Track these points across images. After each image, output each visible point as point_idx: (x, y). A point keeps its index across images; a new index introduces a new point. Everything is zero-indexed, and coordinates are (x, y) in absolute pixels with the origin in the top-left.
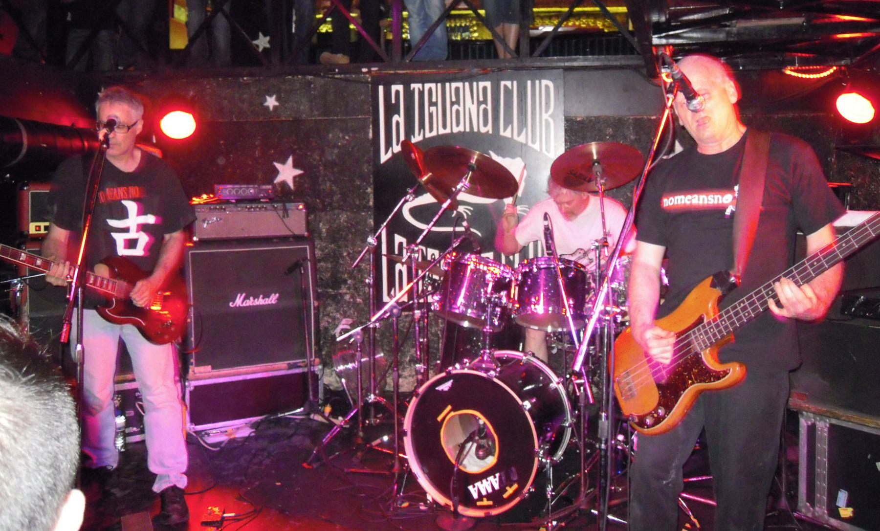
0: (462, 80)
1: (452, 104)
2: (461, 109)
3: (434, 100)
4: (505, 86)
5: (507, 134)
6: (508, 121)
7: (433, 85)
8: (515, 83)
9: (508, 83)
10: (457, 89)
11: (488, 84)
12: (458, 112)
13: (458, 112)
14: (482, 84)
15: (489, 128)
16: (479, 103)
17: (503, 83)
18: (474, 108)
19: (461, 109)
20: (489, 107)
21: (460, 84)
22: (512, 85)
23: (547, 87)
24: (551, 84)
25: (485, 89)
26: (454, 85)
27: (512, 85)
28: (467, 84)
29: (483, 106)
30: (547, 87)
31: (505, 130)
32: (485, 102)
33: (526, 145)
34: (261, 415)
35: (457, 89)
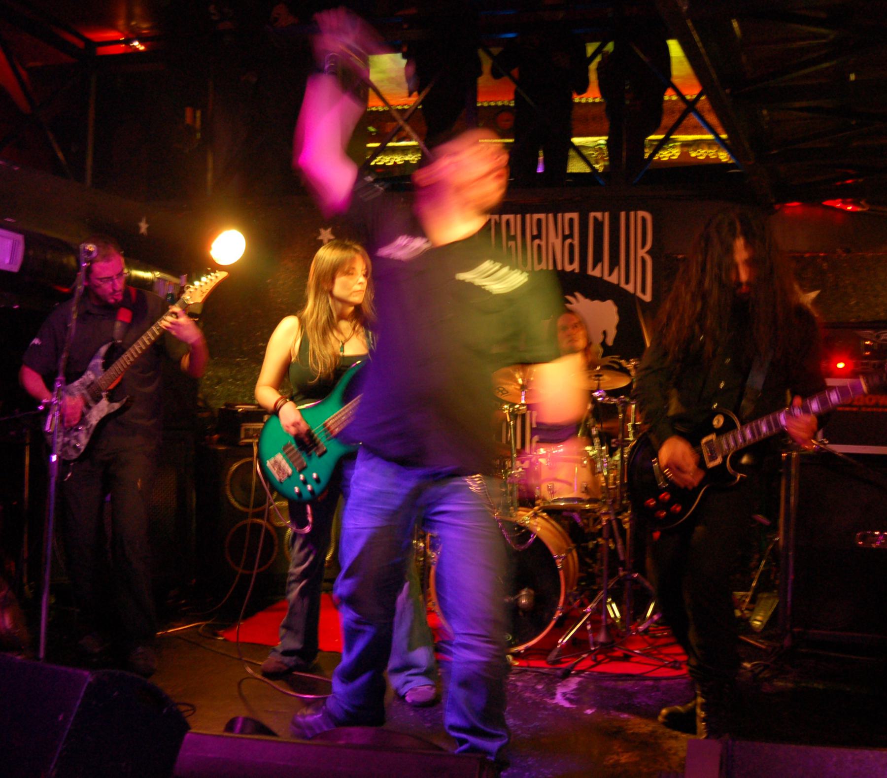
0: (547, 211)
1: (534, 238)
2: (543, 243)
3: (512, 233)
4: (595, 219)
5: (596, 273)
6: (598, 259)
7: (511, 217)
8: (607, 214)
9: (599, 215)
10: (539, 221)
11: (575, 216)
12: (539, 246)
13: (539, 246)
14: (568, 216)
15: (576, 266)
16: (565, 238)
17: (592, 214)
18: (558, 243)
19: (543, 243)
20: (576, 242)
21: (542, 216)
22: (603, 216)
23: (644, 220)
24: (648, 216)
25: (571, 220)
26: (536, 216)
27: (603, 216)
28: (551, 216)
29: (568, 241)
30: (644, 220)
31: (594, 267)
32: (571, 236)
33: (618, 285)
34: (638, 322)
35: (539, 221)
